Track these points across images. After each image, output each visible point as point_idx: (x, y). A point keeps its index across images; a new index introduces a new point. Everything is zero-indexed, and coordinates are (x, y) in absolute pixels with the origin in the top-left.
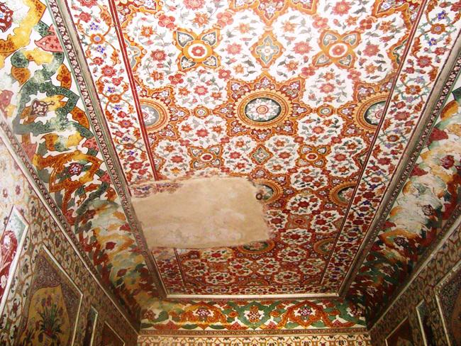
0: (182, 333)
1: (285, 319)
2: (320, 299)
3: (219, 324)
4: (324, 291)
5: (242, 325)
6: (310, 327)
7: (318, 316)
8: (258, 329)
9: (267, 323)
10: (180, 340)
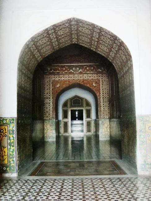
0: (56, 74)
1: (84, 70)
2: (94, 65)
3: (66, 71)
4: (95, 63)
5: (73, 72)
6: (91, 72)
7: (93, 69)
8: (77, 73)
9: (79, 71)
10: (56, 76)
